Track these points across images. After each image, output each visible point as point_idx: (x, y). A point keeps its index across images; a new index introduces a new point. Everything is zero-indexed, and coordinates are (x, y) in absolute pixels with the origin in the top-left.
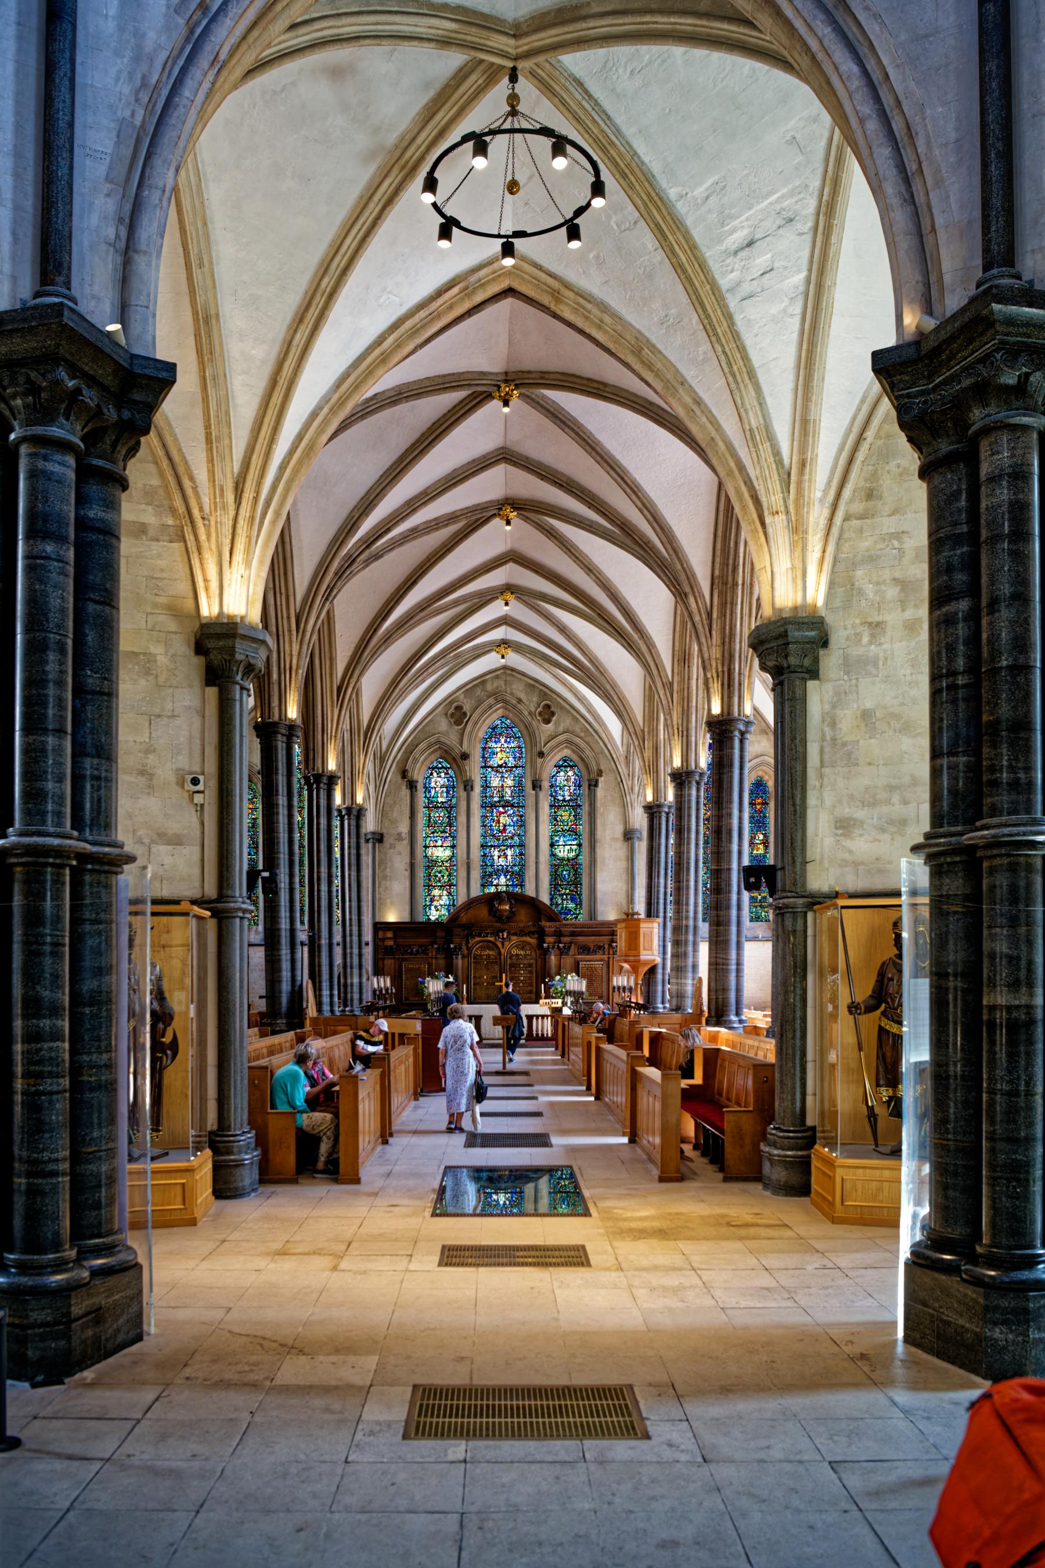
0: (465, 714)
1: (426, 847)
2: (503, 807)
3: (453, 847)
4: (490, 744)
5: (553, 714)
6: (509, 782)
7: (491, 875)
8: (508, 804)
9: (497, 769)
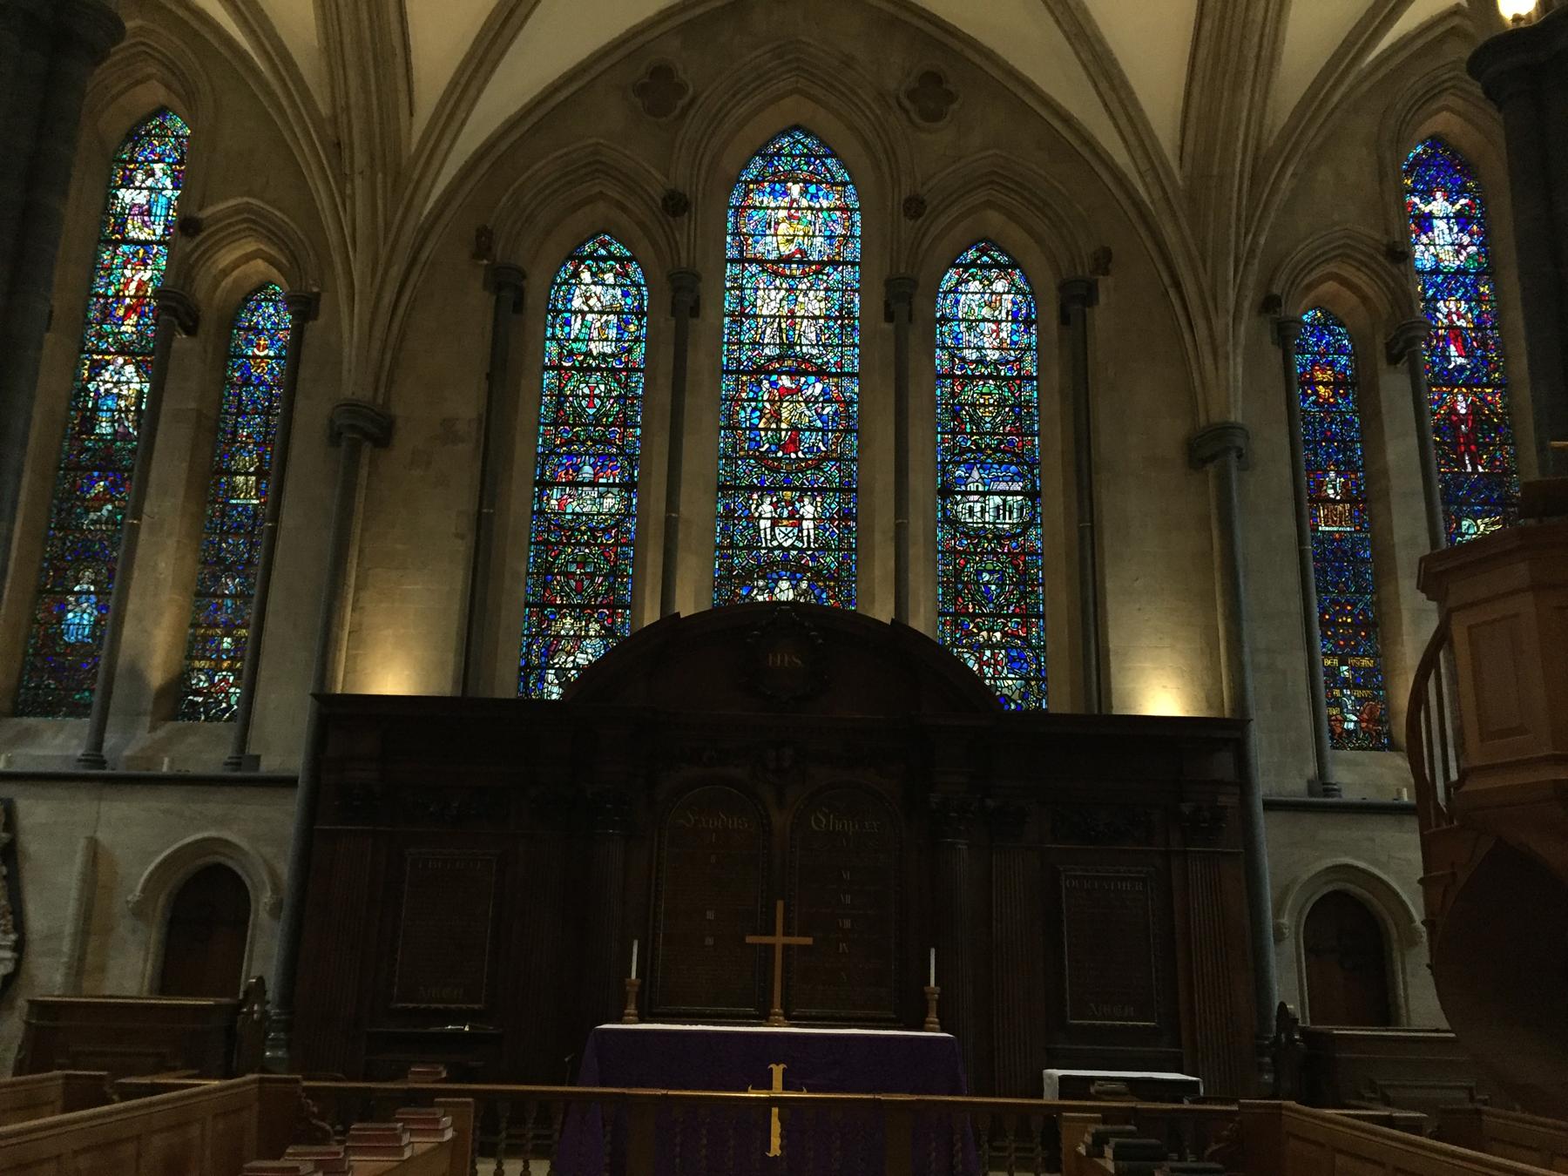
0: (681, 89)
1: (545, 485)
2: (791, 373)
3: (628, 486)
4: (756, 199)
5: (950, 97)
6: (813, 304)
7: (747, 576)
8: (805, 368)
9: (775, 267)
